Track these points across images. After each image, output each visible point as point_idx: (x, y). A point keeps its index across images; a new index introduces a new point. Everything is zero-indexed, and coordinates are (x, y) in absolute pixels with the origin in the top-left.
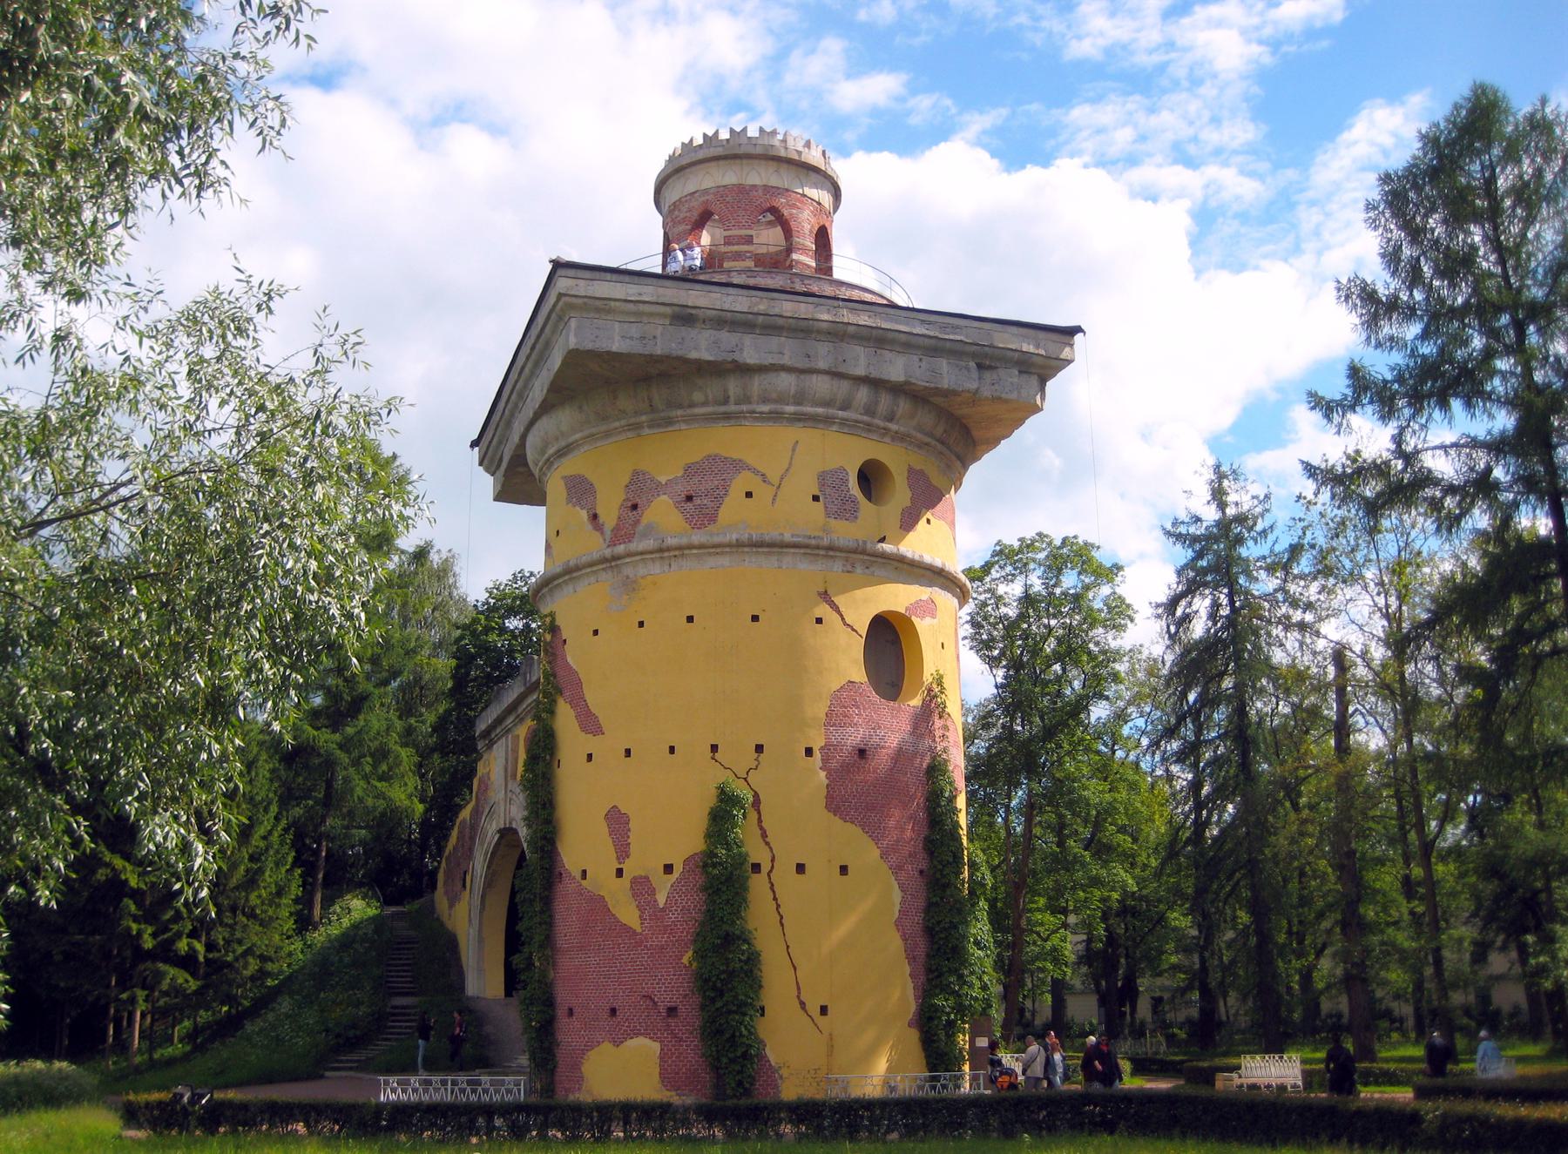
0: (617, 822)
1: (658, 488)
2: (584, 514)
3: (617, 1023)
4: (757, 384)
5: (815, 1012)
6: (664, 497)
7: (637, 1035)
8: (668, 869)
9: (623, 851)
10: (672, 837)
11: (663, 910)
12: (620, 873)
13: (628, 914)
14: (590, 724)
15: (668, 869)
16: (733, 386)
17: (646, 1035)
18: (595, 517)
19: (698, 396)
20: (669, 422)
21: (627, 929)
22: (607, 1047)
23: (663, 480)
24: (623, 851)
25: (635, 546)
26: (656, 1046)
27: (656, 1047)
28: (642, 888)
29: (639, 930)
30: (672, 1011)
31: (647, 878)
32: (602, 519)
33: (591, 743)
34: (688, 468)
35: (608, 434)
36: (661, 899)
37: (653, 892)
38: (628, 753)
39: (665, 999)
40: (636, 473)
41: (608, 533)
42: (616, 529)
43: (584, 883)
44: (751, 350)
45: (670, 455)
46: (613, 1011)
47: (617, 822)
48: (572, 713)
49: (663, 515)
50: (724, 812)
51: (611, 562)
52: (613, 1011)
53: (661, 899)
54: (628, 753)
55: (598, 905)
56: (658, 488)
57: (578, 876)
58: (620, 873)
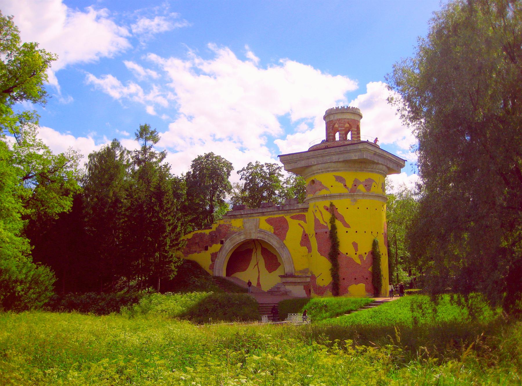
0: (355, 245)
1: (360, 183)
2: (342, 184)
3: (356, 281)
4: (378, 166)
8: (366, 253)
10: (365, 248)
12: (356, 254)
13: (358, 261)
14: (346, 225)
15: (366, 253)
16: (375, 166)
18: (345, 185)
19: (369, 167)
20: (363, 170)
21: (358, 264)
22: (354, 285)
25: (356, 194)
26: (364, 285)
28: (361, 257)
29: (360, 263)
30: (367, 279)
33: (347, 229)
34: (366, 180)
35: (350, 170)
36: (365, 259)
37: (363, 257)
38: (356, 232)
39: (365, 277)
42: (351, 189)
44: (381, 161)
45: (363, 177)
47: (355, 245)
49: (361, 187)
50: (375, 244)
53: (365, 259)
54: (356, 232)
55: (351, 259)
56: (360, 183)
58: (356, 254)
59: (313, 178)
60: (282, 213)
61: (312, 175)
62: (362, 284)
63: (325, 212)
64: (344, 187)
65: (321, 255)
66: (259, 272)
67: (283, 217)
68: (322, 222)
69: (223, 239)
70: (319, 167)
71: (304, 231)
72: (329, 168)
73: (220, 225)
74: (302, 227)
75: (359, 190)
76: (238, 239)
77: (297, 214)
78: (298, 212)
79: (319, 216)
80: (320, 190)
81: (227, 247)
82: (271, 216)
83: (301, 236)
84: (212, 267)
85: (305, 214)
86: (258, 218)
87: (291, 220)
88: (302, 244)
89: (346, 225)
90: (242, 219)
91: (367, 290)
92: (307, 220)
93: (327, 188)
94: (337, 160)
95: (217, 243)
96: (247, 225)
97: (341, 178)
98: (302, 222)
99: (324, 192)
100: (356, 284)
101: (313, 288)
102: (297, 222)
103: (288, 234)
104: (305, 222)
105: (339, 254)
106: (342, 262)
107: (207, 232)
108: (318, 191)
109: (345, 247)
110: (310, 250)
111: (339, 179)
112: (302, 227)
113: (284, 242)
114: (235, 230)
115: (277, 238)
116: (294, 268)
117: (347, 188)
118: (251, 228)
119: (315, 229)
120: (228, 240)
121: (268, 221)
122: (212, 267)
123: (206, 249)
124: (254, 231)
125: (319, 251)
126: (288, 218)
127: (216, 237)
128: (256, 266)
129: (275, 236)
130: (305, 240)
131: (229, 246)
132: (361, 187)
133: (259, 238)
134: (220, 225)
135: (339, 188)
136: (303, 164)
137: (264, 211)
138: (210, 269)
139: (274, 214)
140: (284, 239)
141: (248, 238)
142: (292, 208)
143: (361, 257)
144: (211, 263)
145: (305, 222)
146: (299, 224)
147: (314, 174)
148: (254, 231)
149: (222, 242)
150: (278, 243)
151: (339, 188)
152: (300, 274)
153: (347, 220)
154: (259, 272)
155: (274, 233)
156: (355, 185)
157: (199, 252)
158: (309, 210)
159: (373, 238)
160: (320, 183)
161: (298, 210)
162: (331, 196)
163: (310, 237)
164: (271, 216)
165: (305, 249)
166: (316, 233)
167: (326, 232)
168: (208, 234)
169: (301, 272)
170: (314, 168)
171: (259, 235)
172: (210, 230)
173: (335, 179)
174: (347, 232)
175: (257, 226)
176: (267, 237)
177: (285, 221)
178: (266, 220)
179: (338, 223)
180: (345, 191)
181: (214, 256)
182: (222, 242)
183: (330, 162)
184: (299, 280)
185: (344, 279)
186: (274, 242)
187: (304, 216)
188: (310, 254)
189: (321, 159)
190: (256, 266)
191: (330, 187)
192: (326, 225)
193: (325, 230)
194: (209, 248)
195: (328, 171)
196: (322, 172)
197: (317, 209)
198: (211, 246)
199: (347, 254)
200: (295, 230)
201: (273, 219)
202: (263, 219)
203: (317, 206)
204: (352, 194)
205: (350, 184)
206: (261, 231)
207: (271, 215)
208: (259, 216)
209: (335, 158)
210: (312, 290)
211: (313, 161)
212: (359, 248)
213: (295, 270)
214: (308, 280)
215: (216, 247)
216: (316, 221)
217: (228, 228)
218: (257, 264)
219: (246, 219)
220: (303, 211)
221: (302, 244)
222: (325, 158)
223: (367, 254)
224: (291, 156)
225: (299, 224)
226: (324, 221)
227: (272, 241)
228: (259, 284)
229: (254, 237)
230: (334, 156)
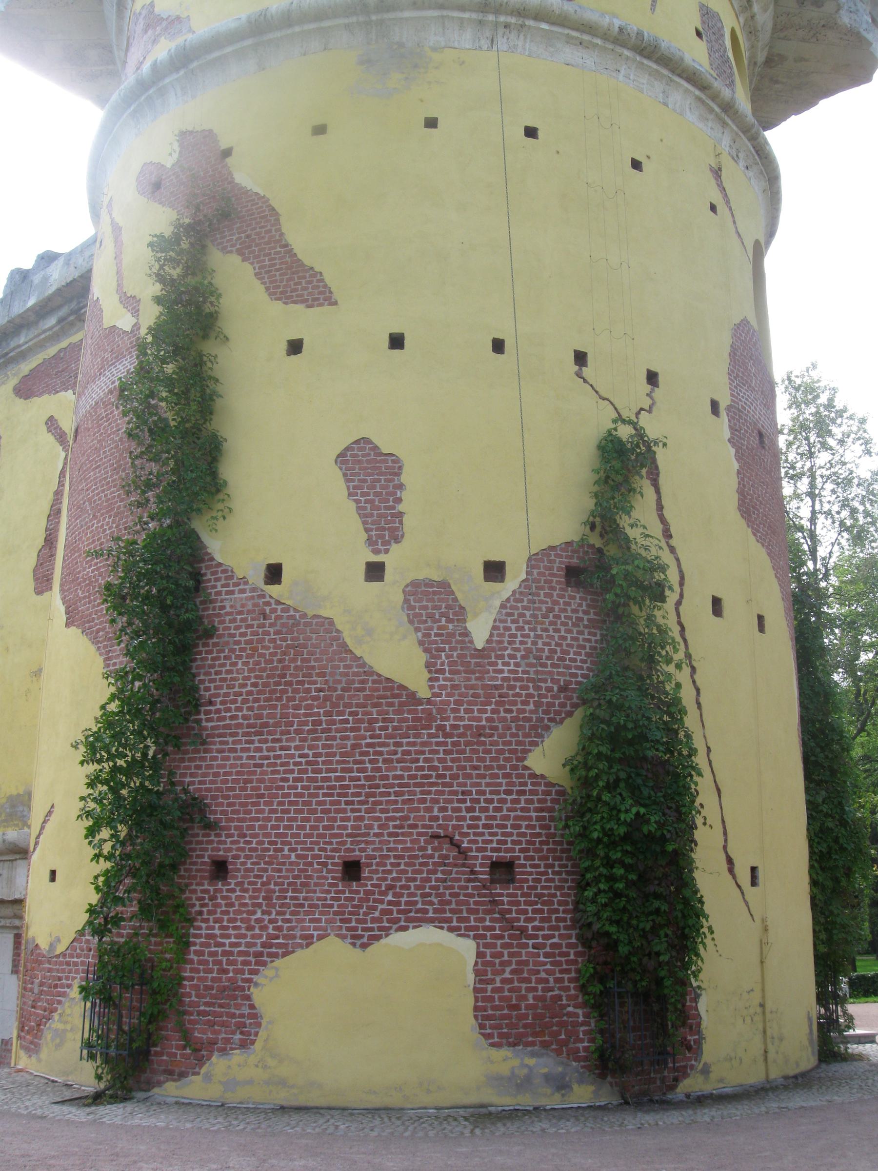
0: (372, 477)
3: (360, 894)
5: (745, 878)
7: (420, 920)
8: (494, 570)
10: (497, 509)
11: (481, 653)
12: (375, 571)
13: (398, 657)
14: (297, 283)
15: (494, 570)
17: (440, 922)
22: (334, 949)
26: (466, 949)
27: (466, 949)
28: (432, 607)
29: (424, 693)
30: (503, 870)
31: (444, 585)
33: (300, 321)
36: (480, 630)
37: (460, 615)
39: (484, 846)
43: (274, 590)
46: (352, 870)
48: (248, 270)
52: (352, 870)
53: (480, 630)
54: (397, 342)
57: (257, 578)
58: (375, 571)
77: (52, 351)
91: (501, 1018)
100: (363, 938)
106: (228, 676)
109: (280, 523)
143: (432, 607)
159: (597, 421)
161: (52, 321)
179: (238, 284)
199: (274, 573)
212: (410, 504)
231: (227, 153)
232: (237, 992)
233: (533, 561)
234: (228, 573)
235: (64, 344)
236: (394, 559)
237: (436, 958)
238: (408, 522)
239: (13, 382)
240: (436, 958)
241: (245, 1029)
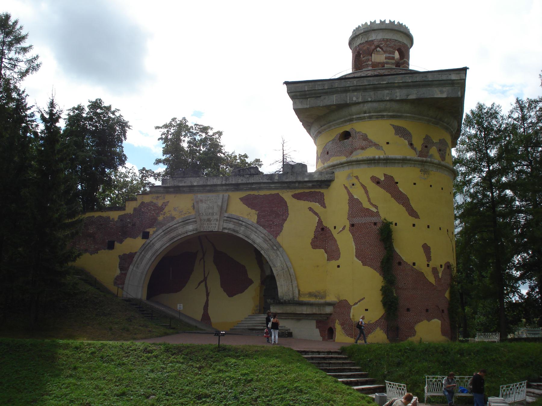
1: (433, 144)
2: (406, 142)
6: (435, 147)
9: (429, 258)
12: (428, 265)
13: (431, 279)
15: (441, 266)
17: (437, 318)
18: (411, 145)
22: (425, 322)
23: (435, 141)
24: (429, 258)
26: (440, 322)
28: (435, 271)
32: (415, 146)
33: (415, 221)
36: (440, 275)
37: (438, 273)
38: (428, 227)
40: (427, 136)
41: (418, 153)
46: (427, 310)
47: (426, 249)
51: (423, 163)
52: (427, 310)
53: (440, 275)
54: (428, 227)
55: (420, 275)
56: (433, 144)
57: (412, 265)
58: (428, 265)
59: (347, 128)
60: (276, 188)
61: (345, 122)
62: (436, 320)
63: (372, 187)
64: (409, 147)
65: (364, 264)
66: (208, 295)
67: (278, 194)
68: (366, 205)
69: (151, 231)
70: (366, 107)
71: (320, 222)
72: (385, 110)
73: (143, 203)
74: (316, 214)
75: (431, 156)
76: (180, 230)
78: (309, 188)
79: (359, 194)
80: (363, 149)
81: (158, 245)
82: (252, 193)
83: (314, 228)
84: (120, 281)
85: (322, 191)
86: (226, 195)
87: (295, 200)
88: (315, 244)
89: (413, 213)
90: (191, 196)
92: (326, 202)
93: (376, 145)
94: (404, 98)
95: (134, 237)
96: (203, 206)
97: (405, 130)
98: (316, 206)
99: (371, 153)
100: (429, 320)
101: (342, 324)
102: (304, 205)
103: (286, 225)
104: (324, 205)
105: (400, 263)
107: (115, 215)
108: (359, 151)
110: (333, 254)
111: (401, 132)
112: (316, 214)
113: (279, 239)
114: (174, 213)
115: (265, 231)
116: (298, 286)
117: (415, 149)
118: (210, 211)
119: (351, 216)
120: (160, 231)
121: (248, 201)
122: (120, 281)
123: (111, 246)
124: (217, 217)
125: (360, 255)
126: (287, 196)
127: (134, 225)
128: (203, 284)
129: (261, 228)
130: (323, 238)
131: (160, 242)
132: (433, 151)
133: (226, 231)
134: (143, 203)
135: (399, 149)
136: (334, 99)
137: (240, 181)
138: (115, 283)
139: (260, 189)
140: (277, 234)
141: (202, 230)
142: (300, 179)
144: (118, 272)
145: (324, 205)
146: (310, 209)
147: (351, 120)
148: (217, 217)
149: (146, 236)
150: (265, 241)
151: (399, 149)
152: (312, 300)
153: (413, 205)
154: (208, 295)
155: (258, 222)
156: (426, 147)
157: (96, 251)
158: (334, 185)
160: (365, 138)
161: (310, 185)
162: (387, 161)
163: (334, 233)
164: (252, 193)
165: (321, 253)
166: (352, 225)
167: (375, 224)
168: (116, 219)
169: (311, 295)
170: (354, 109)
171: (226, 225)
172: (122, 213)
173: (394, 131)
174: (414, 225)
175: (223, 209)
176: (242, 229)
177: (283, 203)
178: (242, 199)
180: (411, 154)
181: (126, 260)
182: (146, 236)
183: (391, 100)
184: (305, 310)
185: (408, 310)
186: (258, 239)
187: (322, 195)
188: (334, 263)
189: (372, 93)
190: (203, 283)
191: (382, 143)
192: (375, 210)
193: (374, 220)
194: (117, 244)
195: (383, 117)
196: (370, 118)
197: (355, 181)
198: (121, 242)
199: (414, 264)
200: (300, 220)
201: (256, 197)
202: (236, 197)
203: (357, 177)
204: (424, 159)
205: (418, 144)
206: (230, 219)
207: (253, 189)
208: (227, 190)
209: (399, 94)
210: (338, 328)
211: (356, 97)
213: (299, 291)
214: (328, 310)
215: (133, 244)
216: (353, 202)
217: (161, 209)
218: (205, 279)
219: (200, 196)
220: (320, 187)
221: (315, 244)
222: (379, 92)
223: (443, 267)
224: (310, 84)
225: (310, 209)
226: (371, 204)
227: (253, 236)
228: (206, 317)
229: (215, 226)
230: (398, 90)
231: (397, 183)
232: (413, 328)
233: (445, 264)
234: (407, 263)
235: (313, 190)
236: (431, 263)
237: (436, 323)
238: (432, 258)
239: (293, 193)
240: (436, 323)
241: (414, 333)
